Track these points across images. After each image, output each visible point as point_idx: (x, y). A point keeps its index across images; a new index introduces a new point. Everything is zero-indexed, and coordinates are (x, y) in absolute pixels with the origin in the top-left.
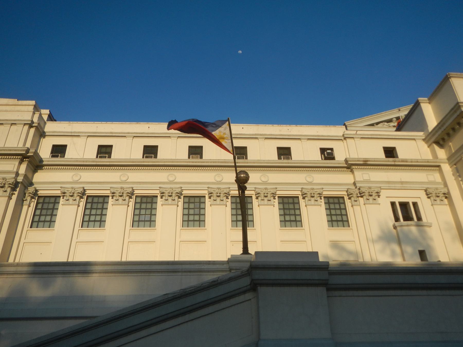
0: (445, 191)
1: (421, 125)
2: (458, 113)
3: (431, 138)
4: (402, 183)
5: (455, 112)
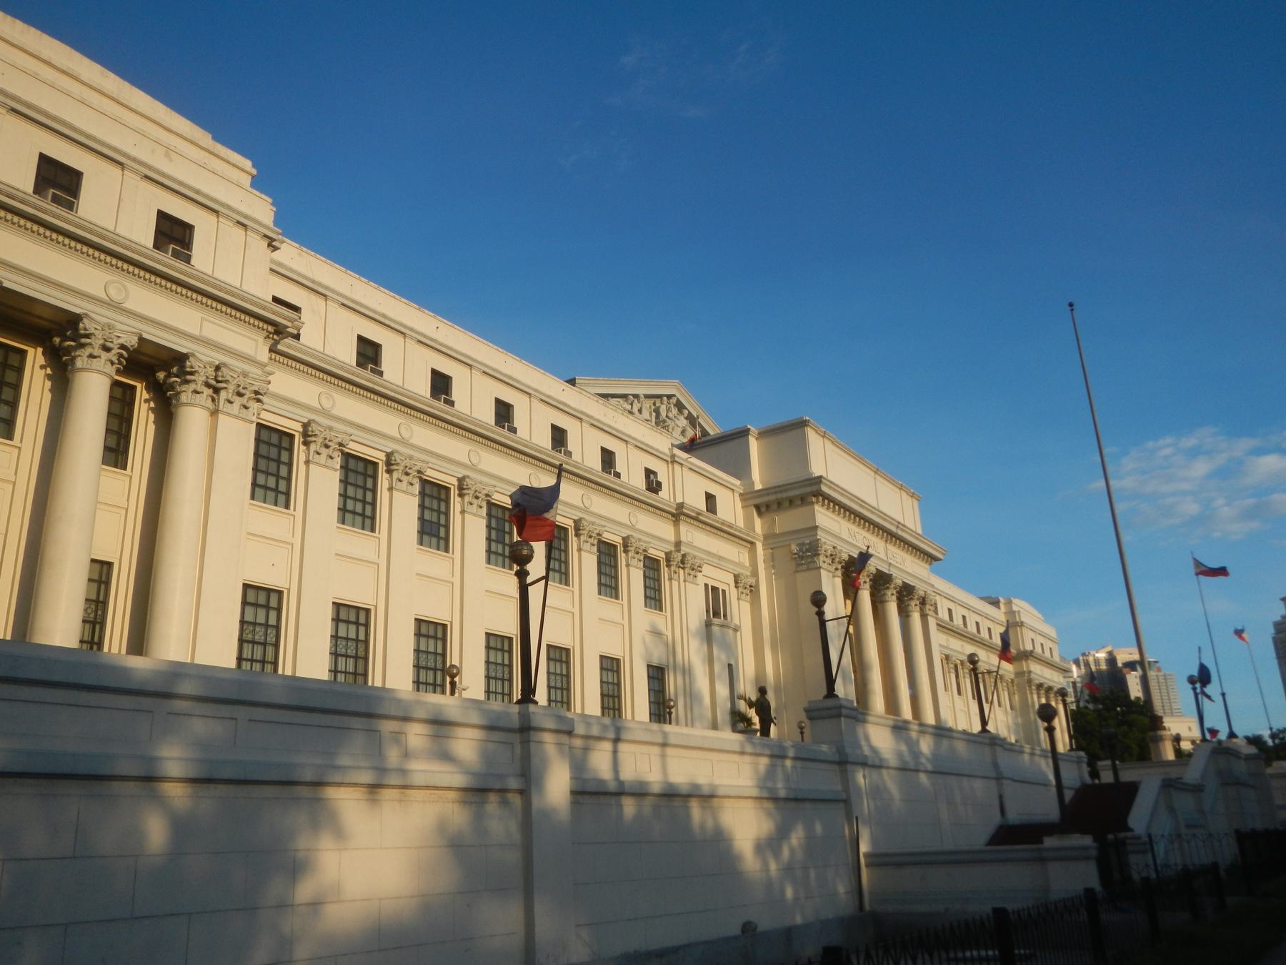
0: (752, 581)
1: (739, 468)
2: (814, 488)
3: (753, 498)
4: (720, 558)
5: (811, 485)
